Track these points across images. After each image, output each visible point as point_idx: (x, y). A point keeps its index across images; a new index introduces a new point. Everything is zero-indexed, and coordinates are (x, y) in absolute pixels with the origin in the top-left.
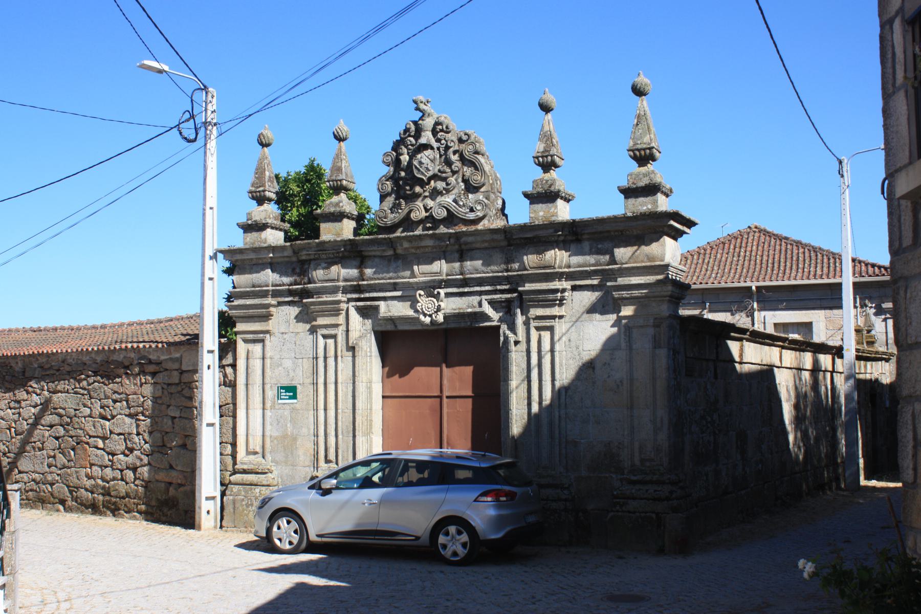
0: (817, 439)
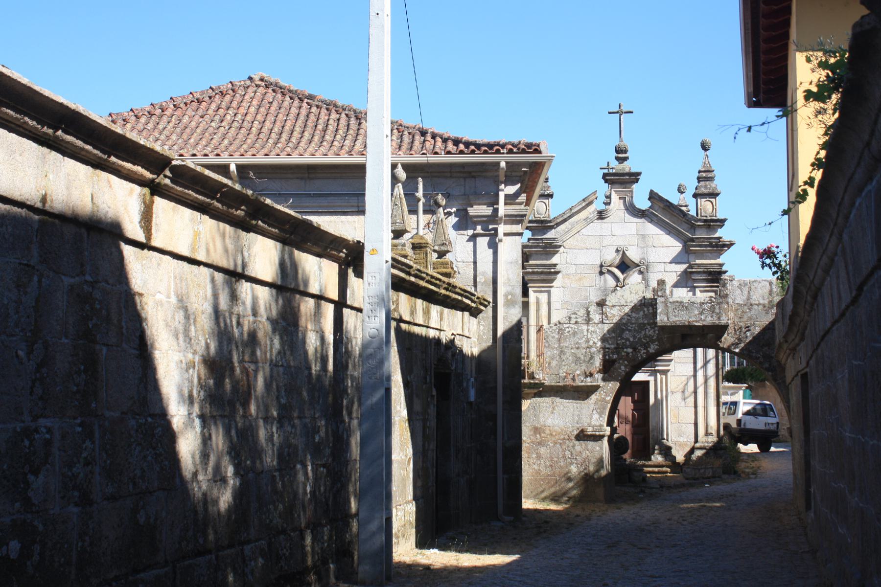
0: (287, 458)
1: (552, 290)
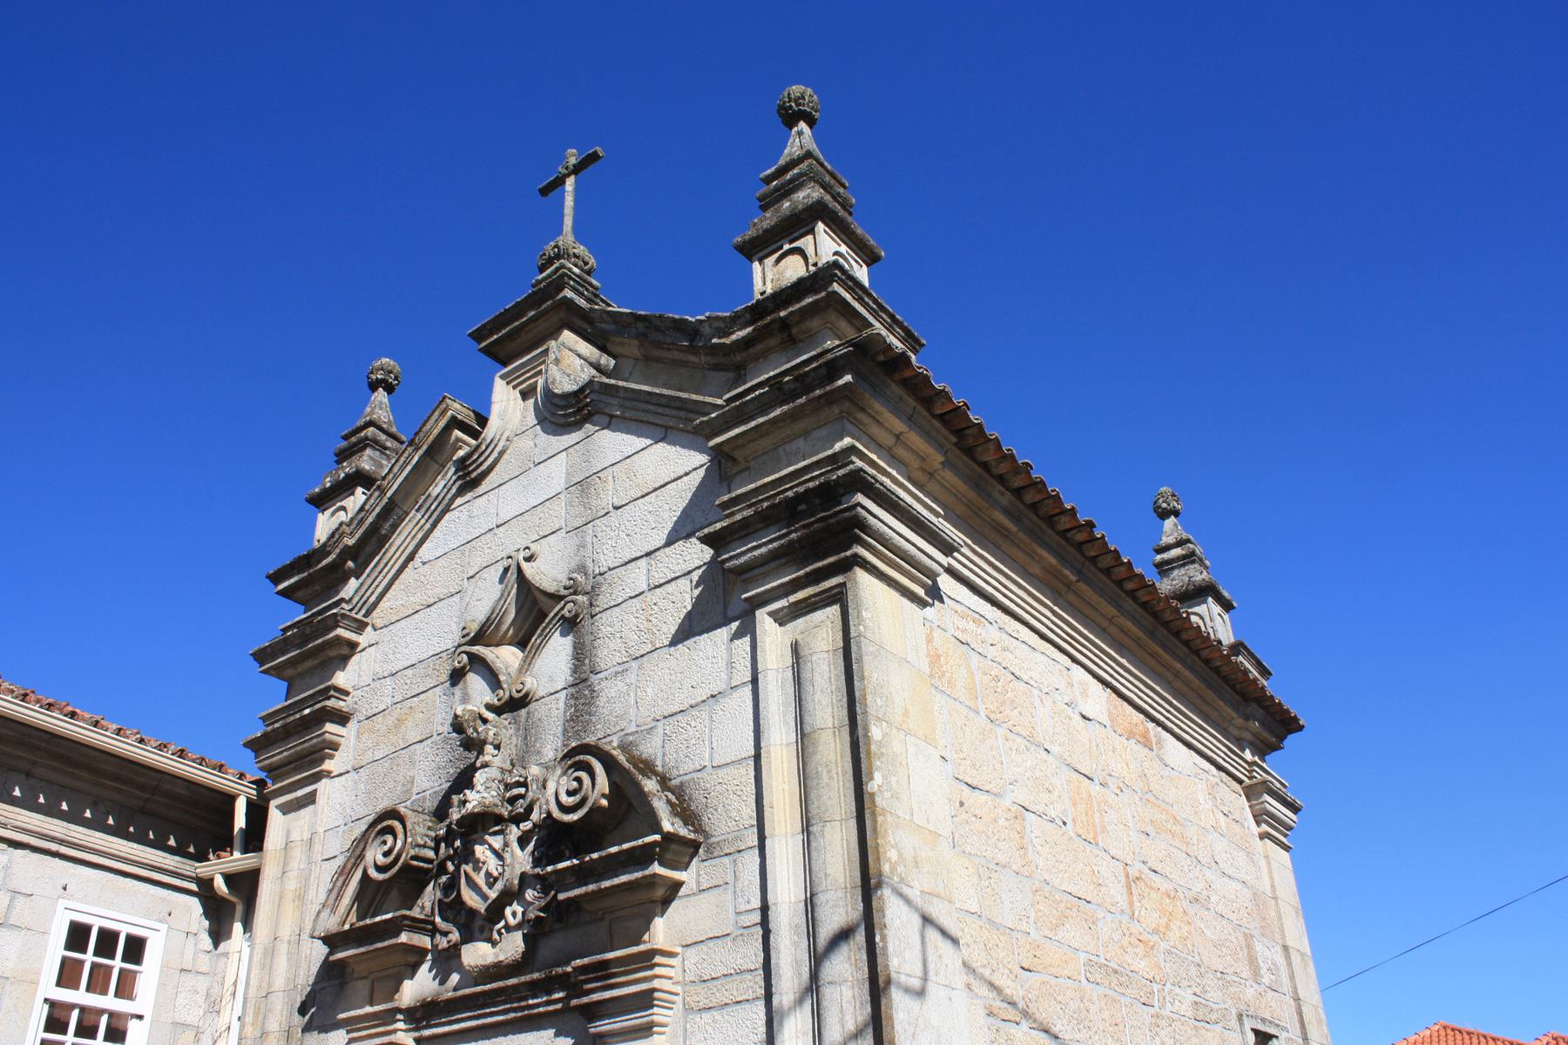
1: (323, 786)
